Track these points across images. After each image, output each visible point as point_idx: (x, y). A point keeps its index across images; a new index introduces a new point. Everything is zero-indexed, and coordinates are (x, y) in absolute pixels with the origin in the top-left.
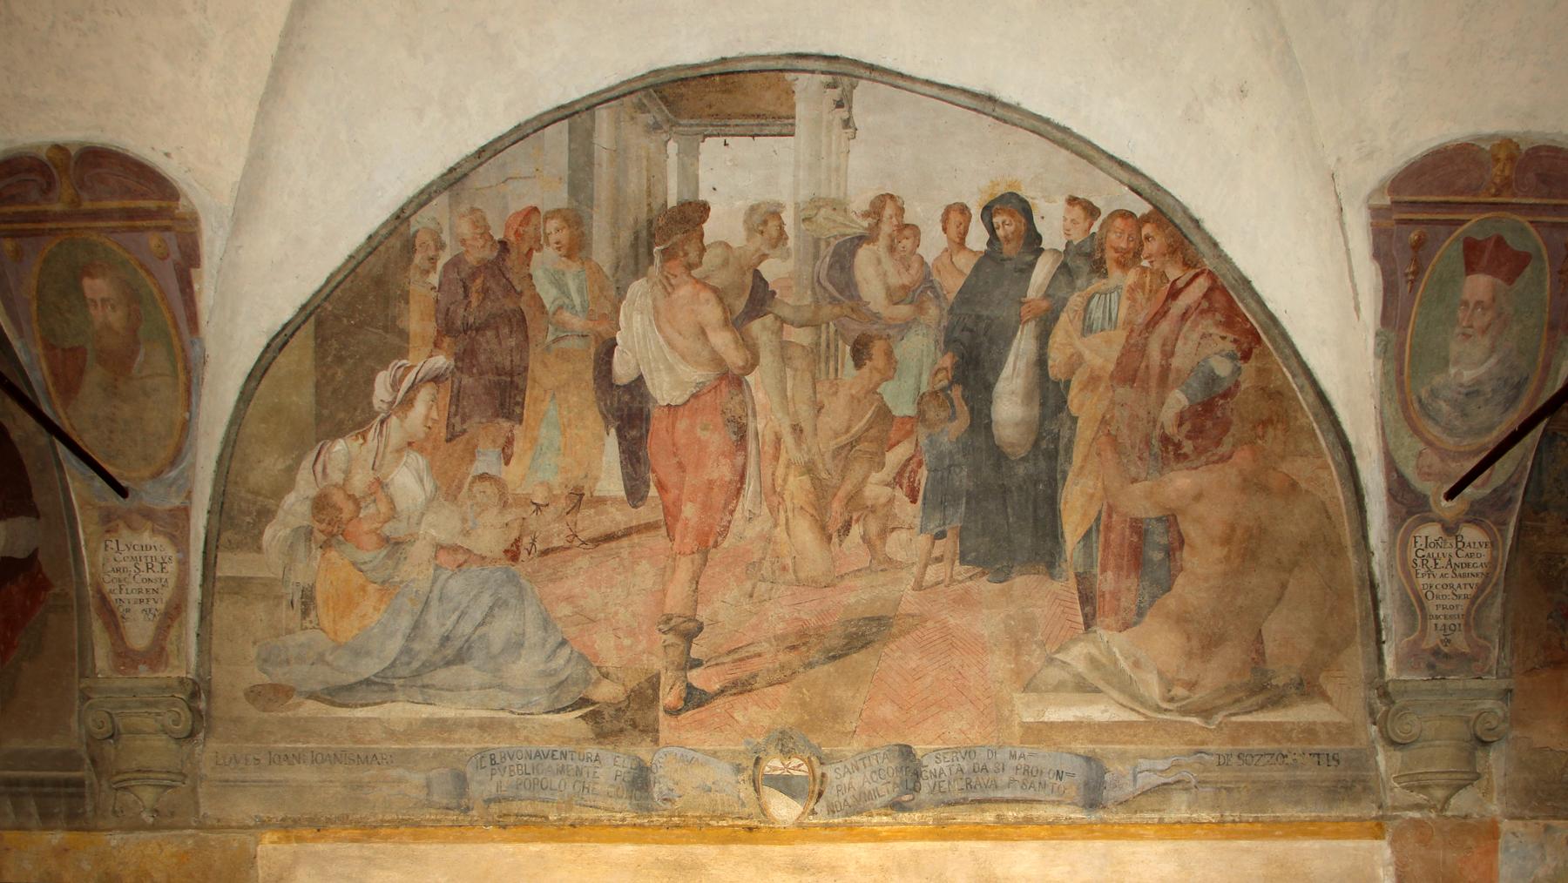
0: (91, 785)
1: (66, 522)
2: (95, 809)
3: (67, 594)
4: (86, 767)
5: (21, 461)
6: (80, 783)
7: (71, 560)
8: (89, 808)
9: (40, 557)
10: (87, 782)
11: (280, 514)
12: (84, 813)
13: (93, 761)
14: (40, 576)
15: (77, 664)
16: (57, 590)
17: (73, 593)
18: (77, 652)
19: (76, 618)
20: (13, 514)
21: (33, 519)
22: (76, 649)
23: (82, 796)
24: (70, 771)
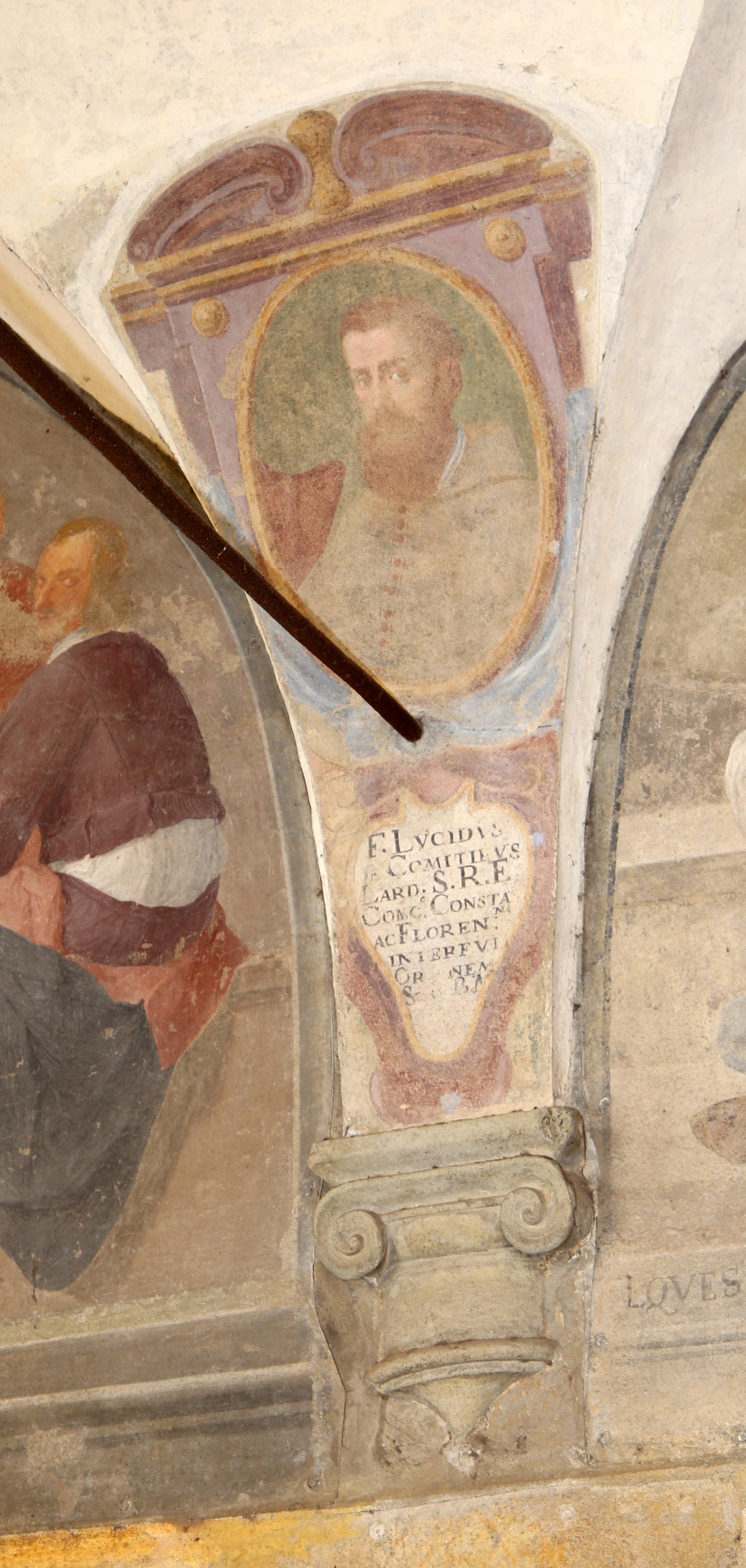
0: (327, 1391)
1: (278, 814)
3: (278, 964)
4: (314, 1349)
5: (189, 712)
7: (288, 892)
8: (320, 1449)
9: (221, 898)
10: (315, 1387)
12: (310, 1461)
13: (331, 1333)
14: (220, 936)
15: (296, 1113)
16: (256, 959)
17: (290, 962)
18: (297, 1087)
19: (296, 1012)
22: (296, 1079)
23: (303, 1422)
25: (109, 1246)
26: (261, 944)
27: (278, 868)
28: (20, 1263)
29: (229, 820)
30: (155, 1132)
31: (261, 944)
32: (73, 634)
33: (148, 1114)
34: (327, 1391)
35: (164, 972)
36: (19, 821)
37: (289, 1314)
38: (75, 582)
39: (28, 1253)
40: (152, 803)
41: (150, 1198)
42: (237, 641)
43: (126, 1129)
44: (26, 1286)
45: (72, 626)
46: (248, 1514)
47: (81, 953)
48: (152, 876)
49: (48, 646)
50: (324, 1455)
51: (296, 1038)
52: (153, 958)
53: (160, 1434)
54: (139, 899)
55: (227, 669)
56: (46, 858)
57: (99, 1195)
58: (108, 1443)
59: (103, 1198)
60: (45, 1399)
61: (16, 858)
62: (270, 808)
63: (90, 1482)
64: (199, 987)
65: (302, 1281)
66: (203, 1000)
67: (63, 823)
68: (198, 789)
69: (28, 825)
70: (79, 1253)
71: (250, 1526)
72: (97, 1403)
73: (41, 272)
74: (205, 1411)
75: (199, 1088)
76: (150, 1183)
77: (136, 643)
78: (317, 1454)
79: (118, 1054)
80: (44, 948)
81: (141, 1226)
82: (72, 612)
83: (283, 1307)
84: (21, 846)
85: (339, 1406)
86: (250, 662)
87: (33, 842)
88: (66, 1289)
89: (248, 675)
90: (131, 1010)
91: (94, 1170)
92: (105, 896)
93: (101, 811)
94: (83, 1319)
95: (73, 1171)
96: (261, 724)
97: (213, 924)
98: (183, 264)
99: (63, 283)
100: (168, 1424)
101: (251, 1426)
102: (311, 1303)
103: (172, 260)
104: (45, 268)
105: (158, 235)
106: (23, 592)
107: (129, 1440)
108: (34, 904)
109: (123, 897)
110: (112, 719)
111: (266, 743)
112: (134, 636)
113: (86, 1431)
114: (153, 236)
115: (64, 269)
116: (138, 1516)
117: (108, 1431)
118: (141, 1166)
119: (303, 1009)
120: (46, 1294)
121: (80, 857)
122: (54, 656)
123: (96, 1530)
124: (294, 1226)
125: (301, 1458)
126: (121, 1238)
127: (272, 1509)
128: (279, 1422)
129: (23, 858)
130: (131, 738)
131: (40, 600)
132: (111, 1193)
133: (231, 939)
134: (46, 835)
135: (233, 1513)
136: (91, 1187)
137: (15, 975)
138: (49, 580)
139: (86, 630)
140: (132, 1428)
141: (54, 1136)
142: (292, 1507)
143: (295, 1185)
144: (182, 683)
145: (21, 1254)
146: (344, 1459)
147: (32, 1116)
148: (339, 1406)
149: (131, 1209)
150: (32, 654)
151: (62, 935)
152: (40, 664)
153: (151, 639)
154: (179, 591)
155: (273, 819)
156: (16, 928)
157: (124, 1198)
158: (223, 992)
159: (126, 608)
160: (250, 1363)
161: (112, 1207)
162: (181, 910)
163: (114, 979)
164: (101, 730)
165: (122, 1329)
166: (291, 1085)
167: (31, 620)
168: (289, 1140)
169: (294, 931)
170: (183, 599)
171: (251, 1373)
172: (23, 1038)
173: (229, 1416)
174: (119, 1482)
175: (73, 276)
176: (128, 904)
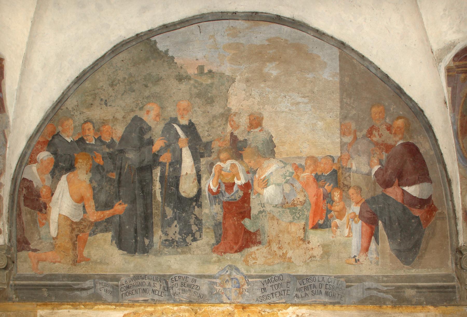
0: (458, 288)
1: (442, 184)
2: (460, 298)
3: (444, 213)
4: (456, 281)
5: (425, 161)
6: (454, 287)
8: (457, 297)
9: (432, 198)
10: (456, 287)
12: (456, 299)
13: (458, 278)
15: (449, 240)
16: (440, 211)
17: (446, 212)
18: (449, 235)
19: (448, 222)
20: (422, 182)
21: (430, 184)
22: (449, 234)
23: (455, 292)
24: (449, 282)
26: (440, 208)
27: (443, 194)
28: (400, 260)
29: (433, 184)
30: (423, 240)
31: (440, 208)
32: (401, 141)
33: (422, 236)
34: (458, 288)
35: (423, 211)
36: (393, 177)
37: (450, 274)
38: (400, 130)
39: (401, 259)
40: (419, 178)
42: (432, 148)
43: (418, 239)
44: (402, 264)
45: (401, 139)
46: (446, 306)
47: (407, 205)
48: (420, 192)
49: (396, 142)
50: (458, 298)
51: (448, 227)
52: (421, 208)
53: (429, 292)
54: (417, 196)
55: (431, 154)
56: (399, 185)
58: (420, 292)
60: (408, 284)
61: (393, 184)
62: (440, 183)
63: (417, 298)
64: (429, 215)
65: (452, 269)
66: (430, 217)
67: (402, 179)
68: (427, 177)
69: (395, 178)
70: (411, 260)
71: (446, 308)
72: (417, 285)
74: (437, 289)
75: (431, 233)
77: (413, 145)
78: (457, 297)
79: (415, 225)
80: (400, 203)
82: (400, 136)
83: (450, 273)
84: (394, 182)
85: (461, 290)
86: (435, 153)
87: (396, 181)
89: (435, 156)
90: (417, 217)
92: (411, 195)
93: (409, 178)
94: (413, 271)
96: (438, 166)
97: (431, 203)
98: (463, 64)
100: (431, 290)
101: (445, 292)
102: (455, 273)
103: (461, 63)
105: (461, 56)
106: (390, 130)
107: (424, 292)
108: (397, 194)
109: (415, 195)
110: (410, 160)
111: (439, 170)
112: (413, 143)
113: (416, 290)
114: (459, 56)
116: (427, 304)
117: (420, 290)
118: (421, 246)
119: (449, 221)
120: (406, 266)
121: (406, 186)
122: (397, 144)
123: (419, 306)
124: (450, 260)
125: (454, 298)
127: (450, 306)
128: (450, 292)
129: (395, 184)
130: (414, 164)
131: (393, 132)
133: (435, 207)
134: (399, 181)
135: (444, 306)
136: (412, 248)
137: (395, 207)
138: (395, 128)
139: (403, 140)
140: (424, 290)
141: (404, 238)
142: (453, 305)
143: (450, 253)
144: (423, 155)
146: (462, 299)
147: (400, 234)
148: (461, 290)
150: (393, 143)
151: (403, 201)
152: (395, 145)
153: (416, 145)
154: (421, 136)
155: (441, 185)
156: (394, 198)
157: (419, 251)
158: (434, 216)
159: (411, 137)
160: (444, 282)
161: (416, 253)
162: (425, 200)
163: (413, 211)
164: (408, 161)
165: (421, 274)
166: (448, 235)
167: (392, 136)
168: (448, 245)
169: (446, 207)
170: (422, 137)
171: (445, 283)
172: (397, 219)
173: (441, 290)
174: (423, 299)
176: (415, 197)
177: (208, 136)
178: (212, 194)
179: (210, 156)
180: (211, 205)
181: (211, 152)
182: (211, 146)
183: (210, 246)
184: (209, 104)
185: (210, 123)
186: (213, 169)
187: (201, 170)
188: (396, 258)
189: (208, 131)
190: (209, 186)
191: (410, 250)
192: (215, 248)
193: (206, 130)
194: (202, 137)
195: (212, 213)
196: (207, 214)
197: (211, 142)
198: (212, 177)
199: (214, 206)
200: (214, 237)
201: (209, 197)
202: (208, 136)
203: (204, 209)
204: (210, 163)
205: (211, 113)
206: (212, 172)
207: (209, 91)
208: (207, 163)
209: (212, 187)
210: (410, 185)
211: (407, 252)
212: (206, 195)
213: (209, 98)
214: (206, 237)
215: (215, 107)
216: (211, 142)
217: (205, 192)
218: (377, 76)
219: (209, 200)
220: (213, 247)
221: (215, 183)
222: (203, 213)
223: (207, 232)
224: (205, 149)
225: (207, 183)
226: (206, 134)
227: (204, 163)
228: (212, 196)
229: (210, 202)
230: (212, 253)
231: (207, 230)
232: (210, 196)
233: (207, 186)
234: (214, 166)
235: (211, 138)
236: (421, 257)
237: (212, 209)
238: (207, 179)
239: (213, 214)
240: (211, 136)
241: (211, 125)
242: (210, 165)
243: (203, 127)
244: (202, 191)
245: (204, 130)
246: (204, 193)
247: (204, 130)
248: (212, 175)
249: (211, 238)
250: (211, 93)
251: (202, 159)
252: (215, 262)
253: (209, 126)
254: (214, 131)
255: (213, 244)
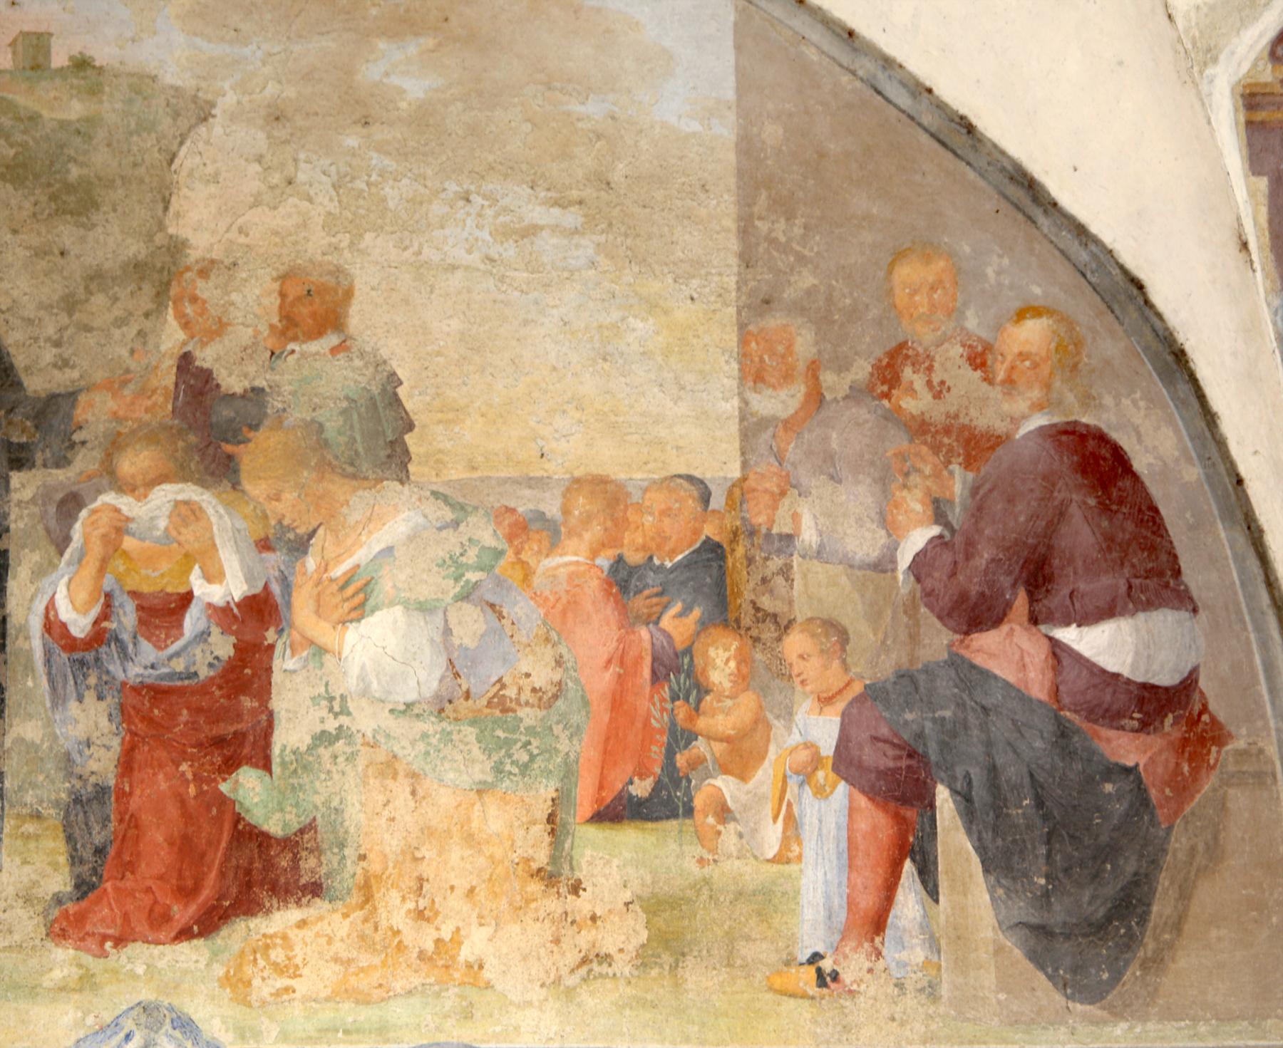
1: (1247, 618)
3: (1261, 751)
5: (1156, 511)
7: (1263, 688)
9: (1202, 683)
11: (1056, 572)
14: (1205, 718)
16: (1241, 744)
20: (1148, 606)
21: (1184, 615)
25: (1134, 973)
26: (1244, 731)
28: (1050, 978)
29: (1203, 615)
30: (1164, 881)
31: (1244, 731)
33: (1155, 863)
35: (1155, 742)
36: (1006, 581)
38: (1035, 366)
39: (1056, 970)
40: (1130, 587)
41: (1167, 936)
42: (1194, 454)
43: (1136, 874)
44: (1059, 998)
45: (1039, 407)
47: (1076, 711)
48: (1137, 653)
49: (1016, 421)
52: (1144, 726)
54: (1126, 672)
55: (1187, 478)
56: (1034, 620)
57: (1118, 928)
59: (1122, 931)
61: (1005, 614)
62: (1239, 612)
64: (1190, 760)
66: (1195, 771)
67: (1048, 591)
68: (1172, 583)
69: (1014, 585)
70: (1105, 976)
73: (1189, 46)
75: (1201, 847)
76: (1166, 923)
79: (1119, 808)
80: (1040, 702)
81: (1162, 960)
82: (1036, 394)
84: (1009, 605)
86: (1208, 477)
87: (1021, 602)
88: (1098, 1004)
89: (1206, 487)
90: (1127, 771)
91: (1109, 905)
92: (1094, 665)
93: (1082, 586)
95: (1090, 903)
97: (1197, 707)
99: (1205, 64)
104: (1194, 44)
106: (983, 364)
108: (1027, 660)
110: (1085, 503)
111: (1229, 552)
115: (1209, 50)
118: (1155, 909)
120: (1079, 1007)
121: (1068, 624)
122: (1023, 431)
126: (1144, 966)
129: (1011, 615)
130: (1105, 524)
131: (1001, 375)
132: (1129, 928)
134: (1032, 599)
136: (1109, 919)
141: (1066, 871)
145: (1050, 970)
149: (1150, 945)
150: (1000, 427)
151: (1056, 692)
152: (1008, 437)
154: (1138, 395)
155: (1242, 621)
156: (1011, 679)
158: (1213, 767)
161: (1130, 942)
162: (1167, 689)
163: (1109, 740)
164: (1074, 510)
167: (995, 393)
169: (1272, 723)
170: (1142, 404)
175: (1215, 60)
176: (1116, 676)
177: (60, 369)
178: (64, 648)
179: (62, 462)
180: (58, 698)
181: (72, 446)
182: (69, 416)
183: (39, 908)
184: (72, 213)
185: (70, 304)
186: (78, 526)
187: (7, 530)
188: (1031, 966)
189: (58, 344)
190: (51, 606)
191: (1098, 929)
192: (65, 914)
193: (48, 339)
194: (27, 369)
195: (62, 741)
196: (32, 747)
197: (72, 396)
198: (69, 564)
199: (73, 705)
200: (62, 859)
201: (48, 662)
202: (55, 365)
203: (16, 721)
204: (59, 496)
205: (78, 257)
206: (67, 539)
207: (72, 153)
208: (44, 496)
209: (65, 612)
210: (1086, 619)
211: (1085, 935)
212: (30, 652)
213: (69, 188)
214: (18, 860)
215: (100, 229)
216: (72, 396)
217: (27, 638)
218: (919, 124)
219: (49, 674)
220: (56, 912)
221: (82, 596)
222: (8, 742)
223: (27, 837)
224: (37, 427)
225: (37, 590)
226: (49, 355)
227: (27, 494)
228: (62, 657)
229: (53, 688)
230: (49, 944)
231: (30, 828)
232: (55, 658)
233: (40, 607)
234: (84, 514)
235: (75, 374)
236: (1156, 963)
237: (64, 722)
238: (39, 572)
239: (66, 745)
240: (73, 367)
241: (77, 316)
242: (62, 503)
243: (30, 321)
244: (11, 631)
245: (36, 339)
246: (20, 643)
247: (36, 339)
248: (67, 555)
249: (49, 870)
250: (82, 165)
251: (16, 478)
252: (62, 989)
253: (63, 318)
254: (92, 342)
255: (58, 900)
